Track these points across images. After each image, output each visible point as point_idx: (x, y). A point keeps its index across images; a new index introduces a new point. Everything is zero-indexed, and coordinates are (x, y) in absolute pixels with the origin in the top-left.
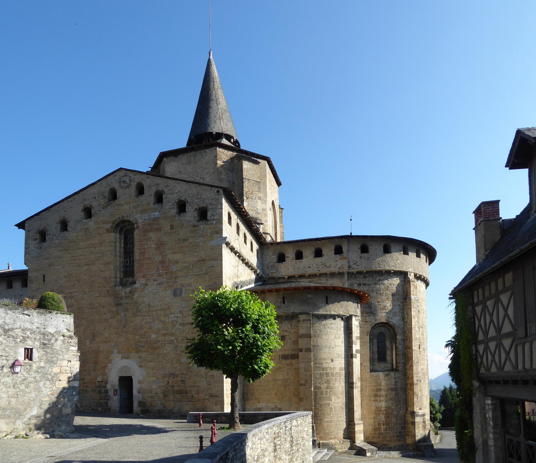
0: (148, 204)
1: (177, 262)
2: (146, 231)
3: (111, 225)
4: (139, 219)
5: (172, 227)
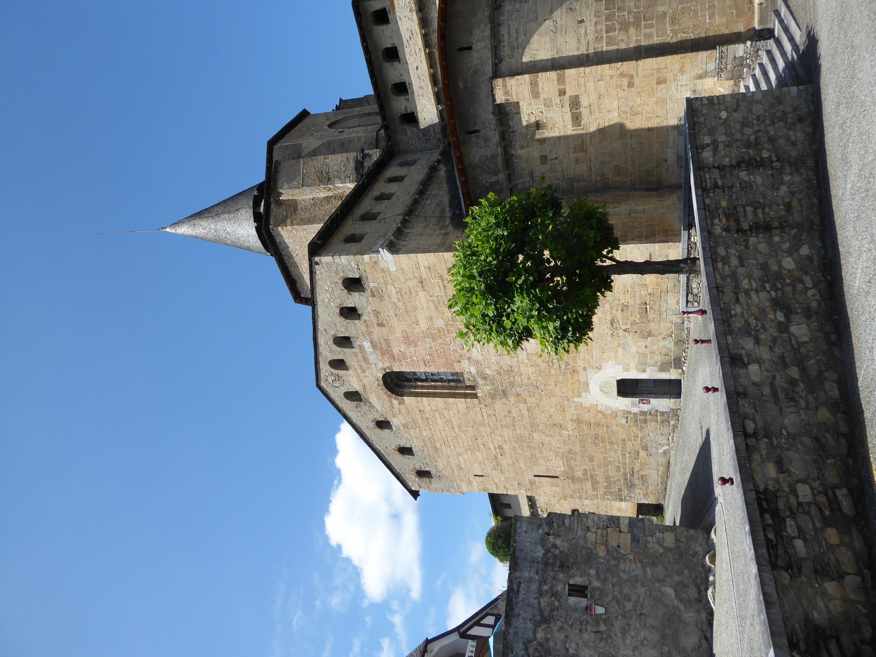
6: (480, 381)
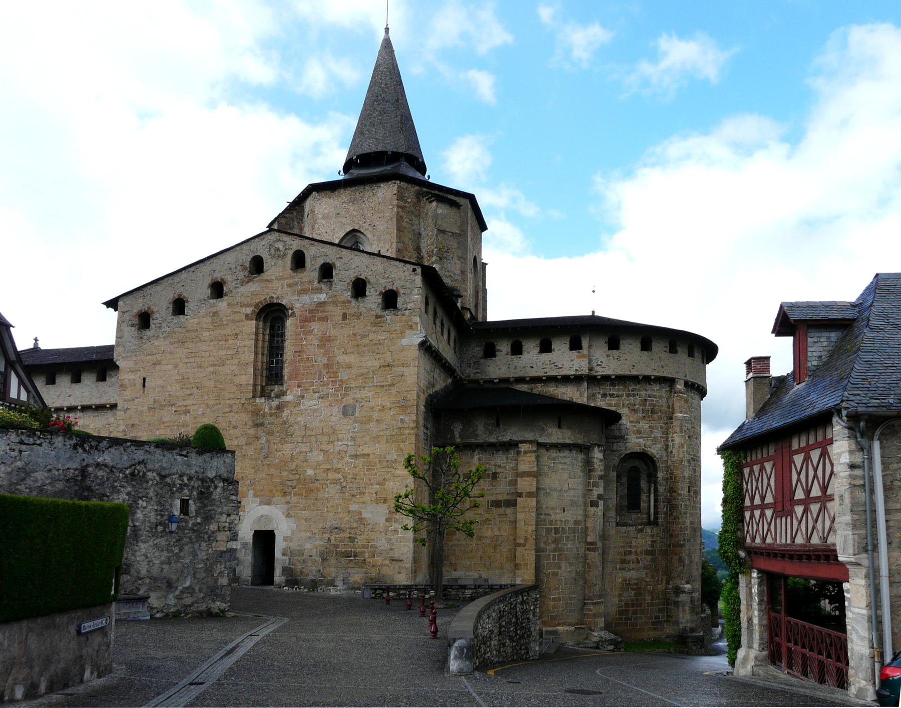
0: (311, 282)
1: (349, 367)
2: (305, 320)
3: (252, 309)
5: (345, 317)
6: (275, 403)
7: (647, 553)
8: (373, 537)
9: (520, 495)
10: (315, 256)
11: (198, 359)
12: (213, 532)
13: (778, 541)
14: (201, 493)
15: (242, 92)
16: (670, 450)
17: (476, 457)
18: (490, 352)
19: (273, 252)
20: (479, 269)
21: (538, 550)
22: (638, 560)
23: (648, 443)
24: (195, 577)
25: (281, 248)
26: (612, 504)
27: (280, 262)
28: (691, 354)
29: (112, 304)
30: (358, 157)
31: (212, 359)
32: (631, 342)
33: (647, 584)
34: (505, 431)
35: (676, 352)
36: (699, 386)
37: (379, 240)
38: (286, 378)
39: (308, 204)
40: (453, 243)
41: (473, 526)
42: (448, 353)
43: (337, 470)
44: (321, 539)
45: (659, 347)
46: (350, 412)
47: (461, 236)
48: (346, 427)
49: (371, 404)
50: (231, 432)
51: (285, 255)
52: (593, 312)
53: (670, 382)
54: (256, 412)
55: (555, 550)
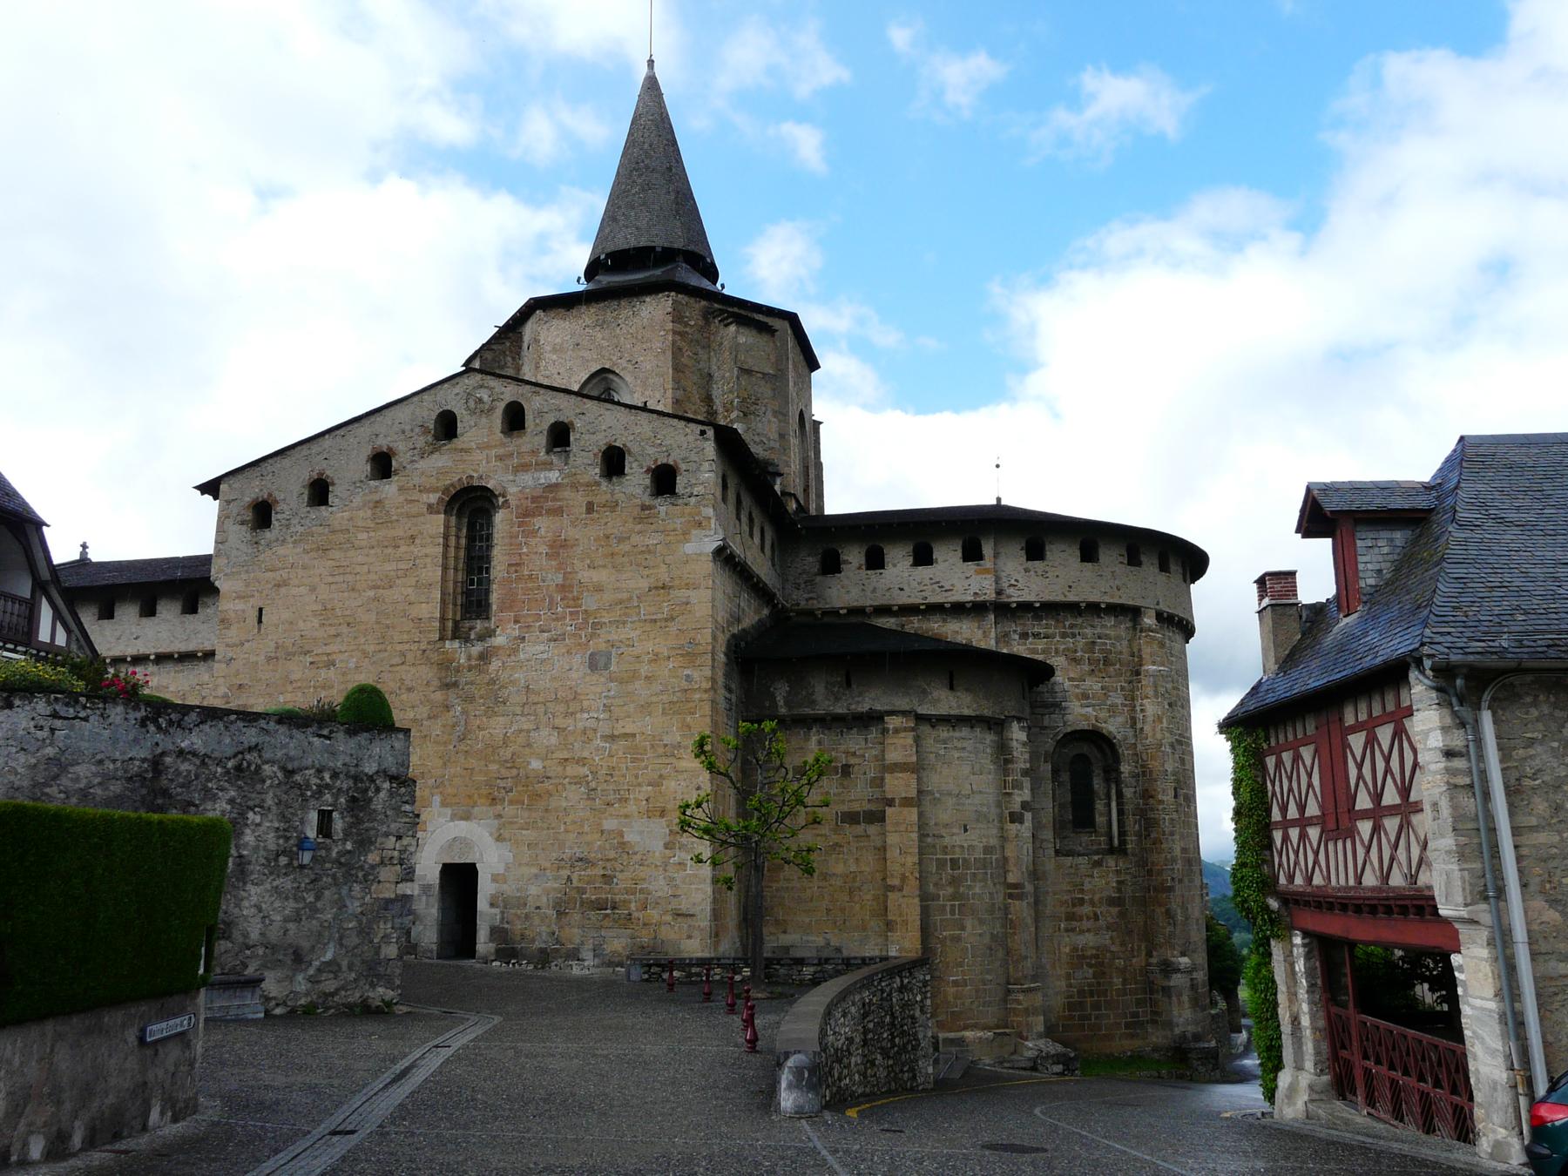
1: (599, 589)
3: (438, 495)
4: (512, 484)
5: (590, 508)
6: (477, 649)
7: (1112, 902)
8: (642, 875)
9: (890, 803)
10: (541, 412)
11: (349, 578)
12: (373, 867)
13: (1334, 882)
14: (353, 800)
15: (422, 159)
16: (1139, 726)
17: (814, 739)
18: (832, 565)
19: (472, 404)
20: (809, 430)
21: (925, 898)
22: (1095, 914)
23: (1103, 715)
24: (341, 945)
25: (486, 398)
26: (1047, 816)
27: (484, 420)
28: (1164, 568)
29: (210, 488)
30: (608, 255)
31: (373, 576)
32: (1063, 547)
33: (1115, 956)
34: (860, 694)
35: (1139, 564)
36: (1181, 620)
37: (644, 384)
38: (494, 607)
39: (529, 330)
40: (765, 390)
41: (813, 856)
42: (761, 566)
43: (582, 761)
44: (556, 879)
45: (1111, 557)
46: (601, 664)
47: (777, 378)
48: (595, 688)
49: (637, 651)
50: (404, 697)
51: (491, 409)
52: (999, 499)
53: (1132, 613)
54: (446, 665)
55: (954, 897)
